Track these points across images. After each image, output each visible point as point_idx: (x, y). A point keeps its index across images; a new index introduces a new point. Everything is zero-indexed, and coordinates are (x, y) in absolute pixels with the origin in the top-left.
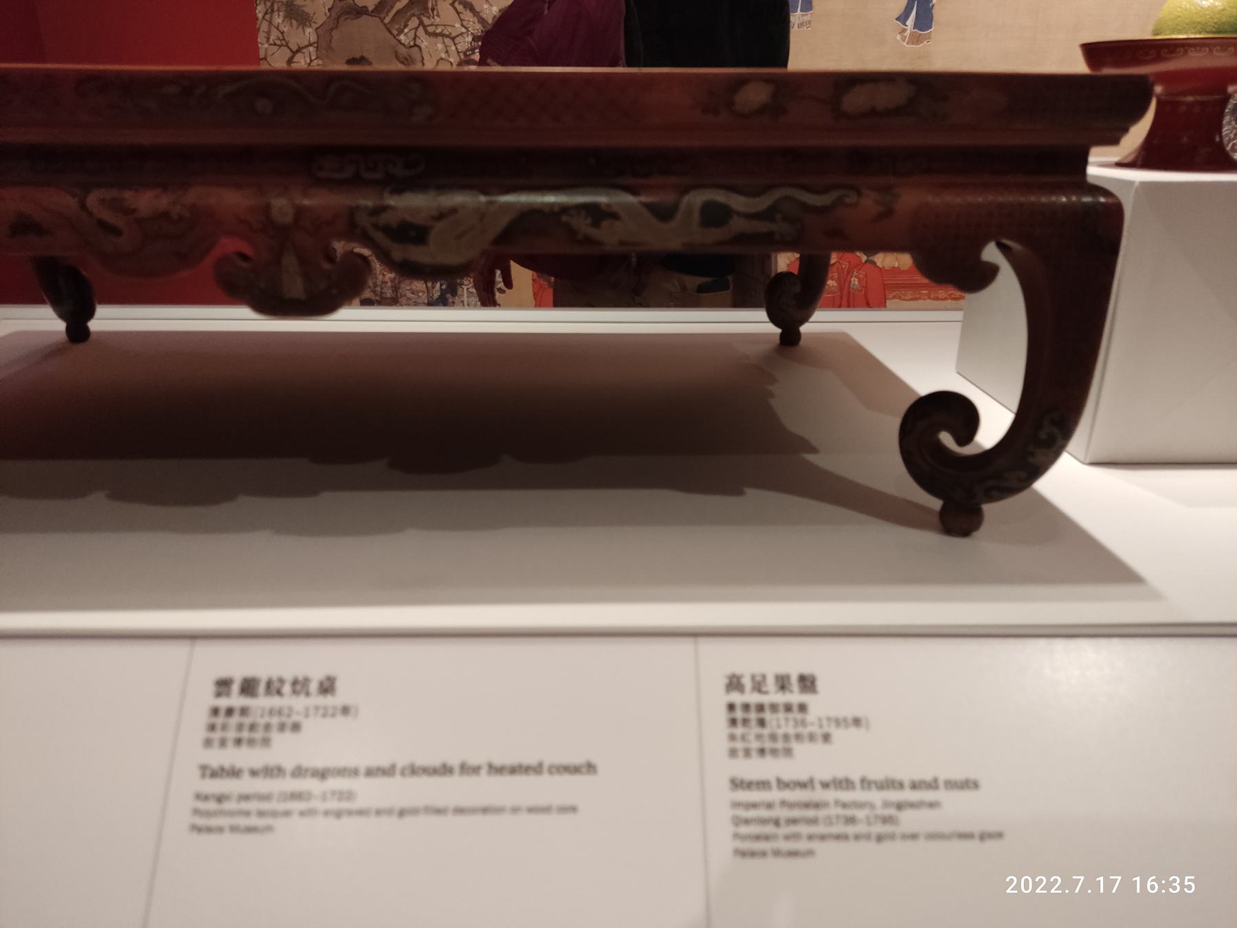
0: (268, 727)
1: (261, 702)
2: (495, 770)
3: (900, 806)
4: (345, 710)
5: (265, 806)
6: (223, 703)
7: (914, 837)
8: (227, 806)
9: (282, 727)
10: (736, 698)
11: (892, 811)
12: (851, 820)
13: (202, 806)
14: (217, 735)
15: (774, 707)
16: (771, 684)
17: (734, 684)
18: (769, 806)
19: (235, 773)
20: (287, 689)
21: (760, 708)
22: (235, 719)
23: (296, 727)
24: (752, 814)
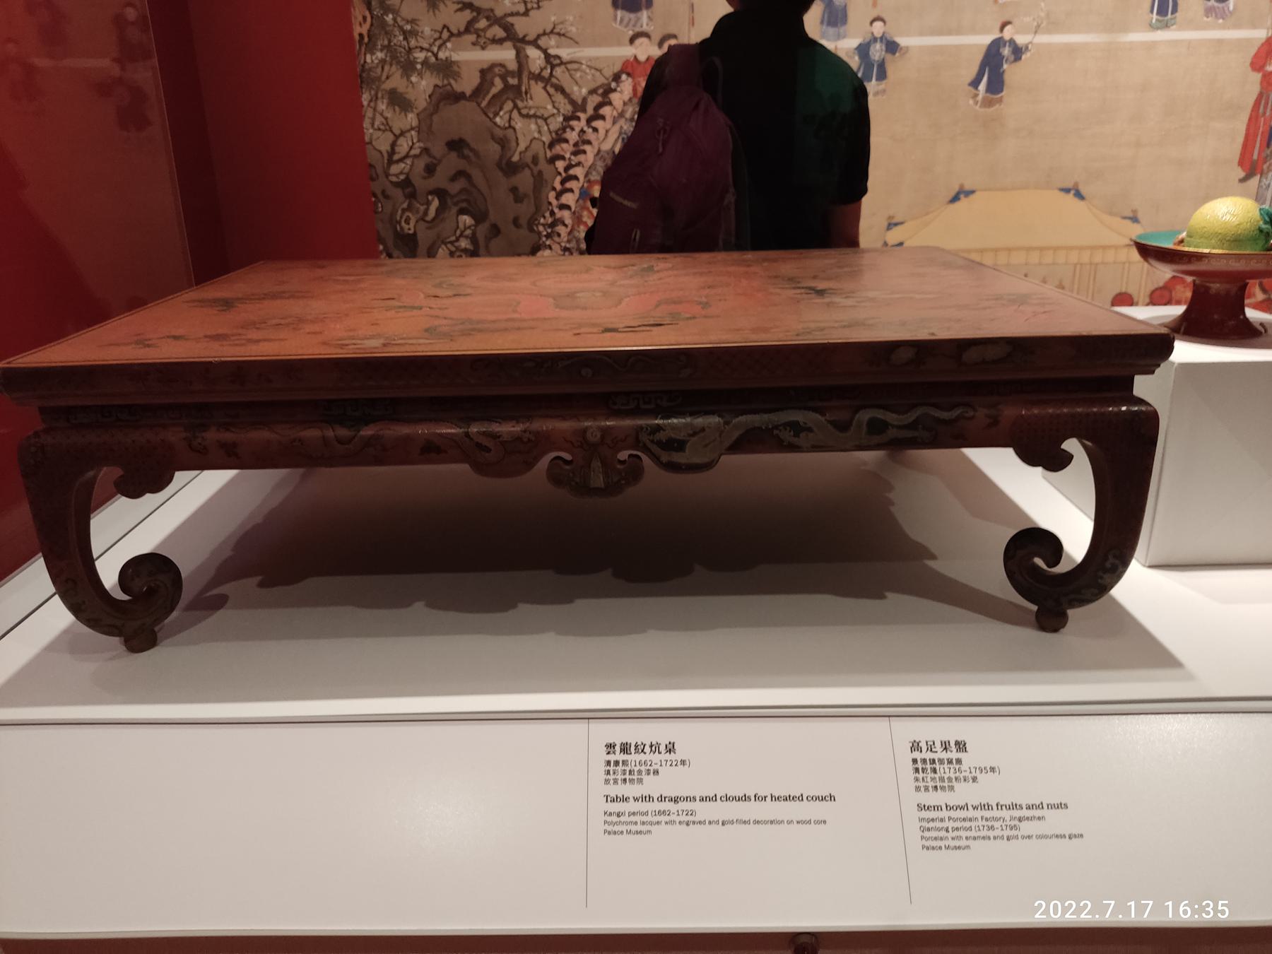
0: (640, 772)
1: (633, 757)
2: (775, 798)
3: (1020, 820)
4: (683, 762)
5: (644, 818)
6: (612, 758)
7: (1029, 837)
8: (622, 819)
9: (648, 772)
10: (917, 755)
11: (1016, 822)
12: (992, 828)
13: (609, 819)
14: (611, 777)
15: (941, 761)
16: (938, 747)
17: (915, 746)
18: (942, 820)
19: (625, 799)
20: (647, 749)
21: (933, 761)
22: (620, 768)
23: (656, 772)
24: (931, 825)
